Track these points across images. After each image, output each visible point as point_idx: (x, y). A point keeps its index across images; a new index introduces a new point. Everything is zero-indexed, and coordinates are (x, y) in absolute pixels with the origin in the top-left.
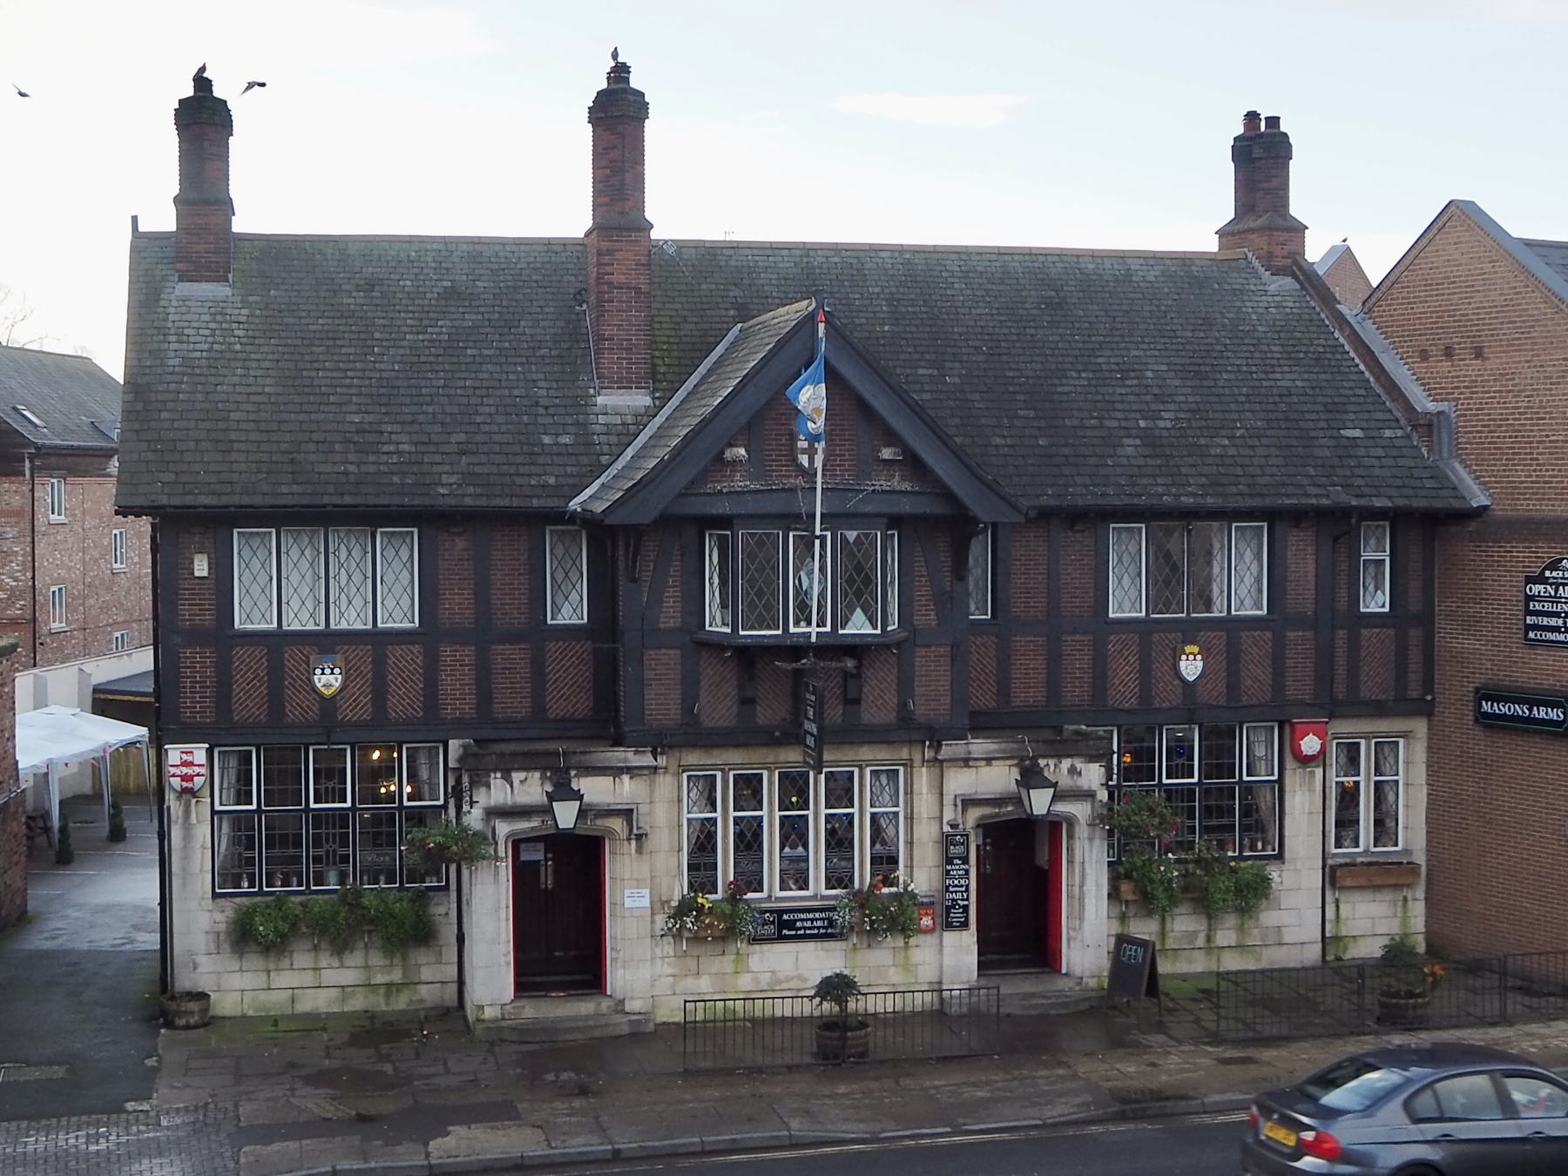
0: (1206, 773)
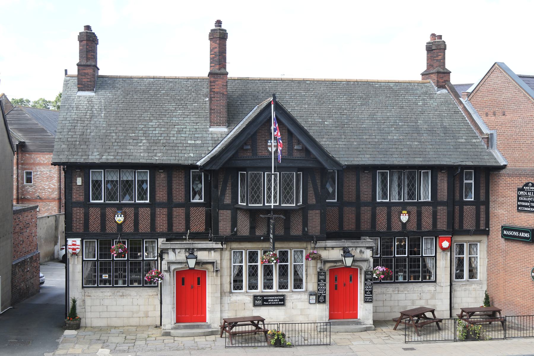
0: (410, 253)
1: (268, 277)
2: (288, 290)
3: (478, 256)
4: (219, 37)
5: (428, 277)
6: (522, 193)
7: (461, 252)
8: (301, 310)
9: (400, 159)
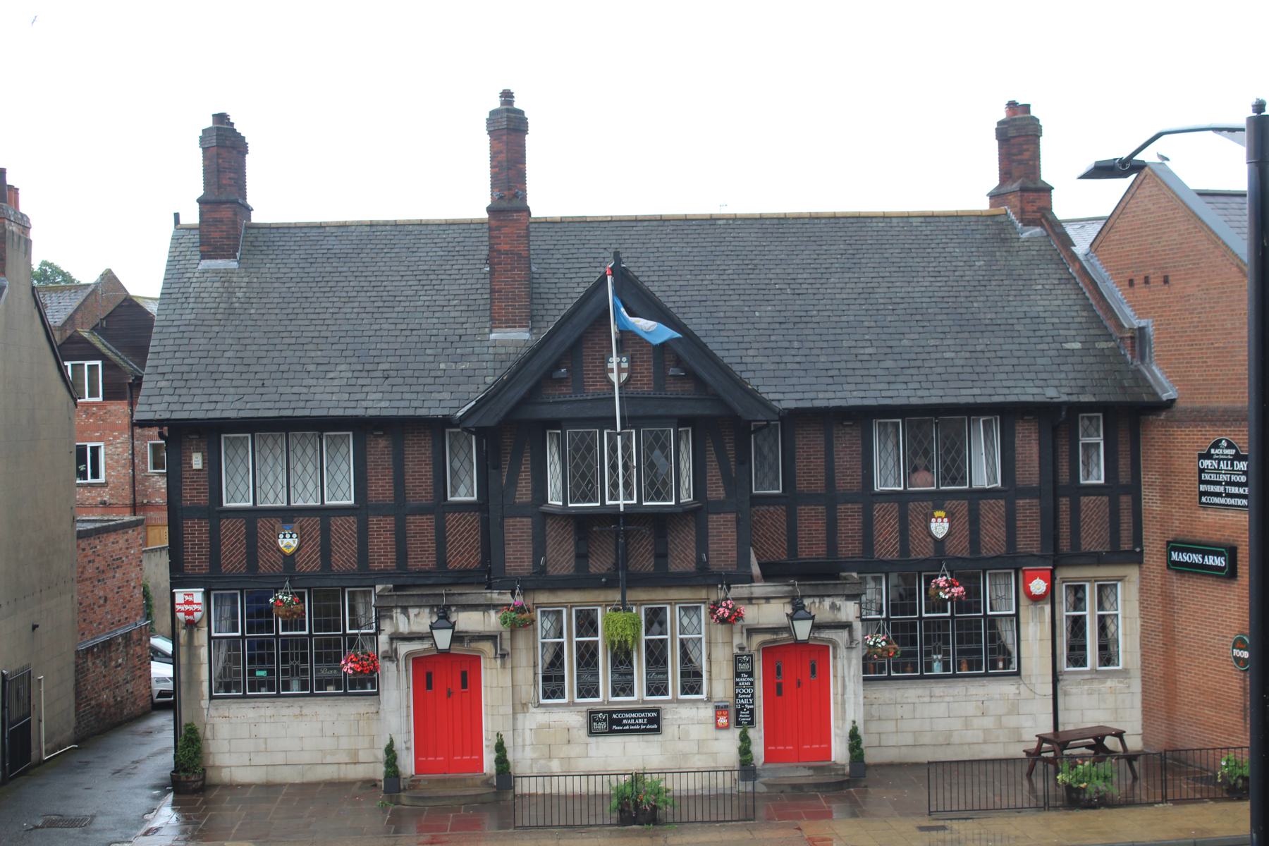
1: (623, 669)
2: (669, 697)
3: (1120, 612)
4: (508, 129)
5: (1001, 665)
6: (1206, 463)
7: (1078, 602)
8: (700, 742)
9: (926, 393)
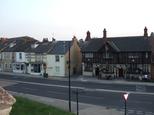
0: (135, 67)
4: (105, 32)
